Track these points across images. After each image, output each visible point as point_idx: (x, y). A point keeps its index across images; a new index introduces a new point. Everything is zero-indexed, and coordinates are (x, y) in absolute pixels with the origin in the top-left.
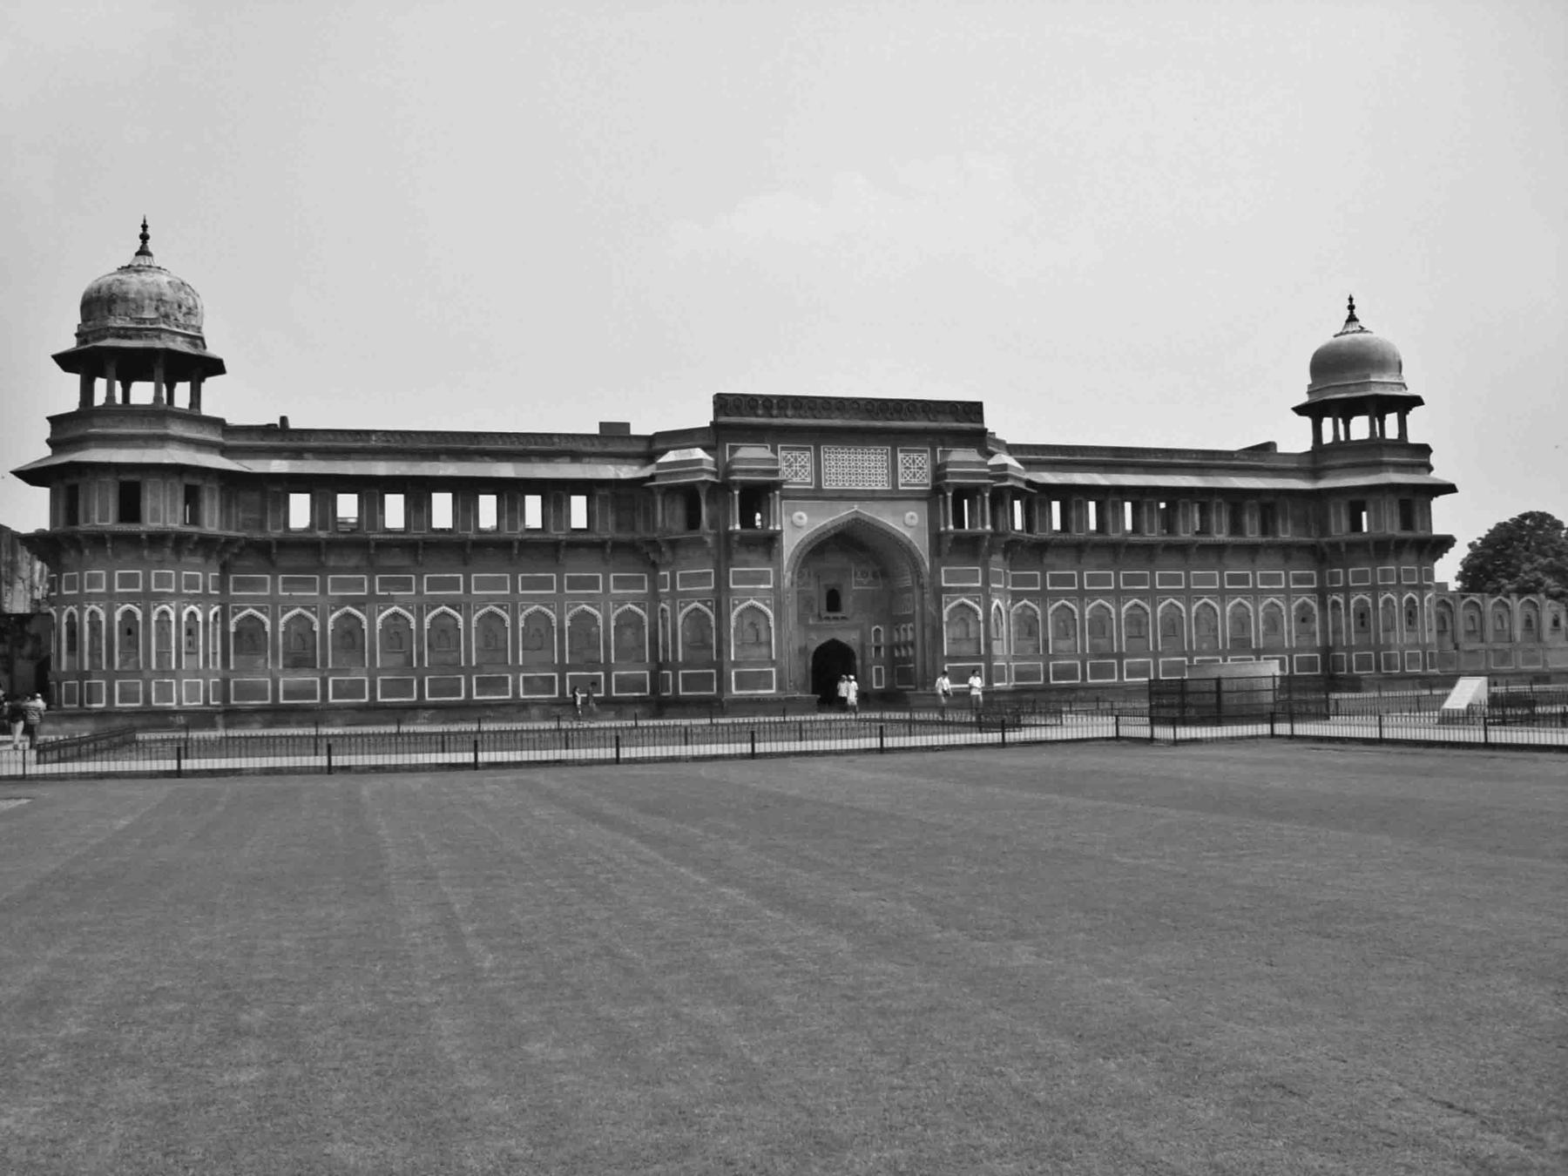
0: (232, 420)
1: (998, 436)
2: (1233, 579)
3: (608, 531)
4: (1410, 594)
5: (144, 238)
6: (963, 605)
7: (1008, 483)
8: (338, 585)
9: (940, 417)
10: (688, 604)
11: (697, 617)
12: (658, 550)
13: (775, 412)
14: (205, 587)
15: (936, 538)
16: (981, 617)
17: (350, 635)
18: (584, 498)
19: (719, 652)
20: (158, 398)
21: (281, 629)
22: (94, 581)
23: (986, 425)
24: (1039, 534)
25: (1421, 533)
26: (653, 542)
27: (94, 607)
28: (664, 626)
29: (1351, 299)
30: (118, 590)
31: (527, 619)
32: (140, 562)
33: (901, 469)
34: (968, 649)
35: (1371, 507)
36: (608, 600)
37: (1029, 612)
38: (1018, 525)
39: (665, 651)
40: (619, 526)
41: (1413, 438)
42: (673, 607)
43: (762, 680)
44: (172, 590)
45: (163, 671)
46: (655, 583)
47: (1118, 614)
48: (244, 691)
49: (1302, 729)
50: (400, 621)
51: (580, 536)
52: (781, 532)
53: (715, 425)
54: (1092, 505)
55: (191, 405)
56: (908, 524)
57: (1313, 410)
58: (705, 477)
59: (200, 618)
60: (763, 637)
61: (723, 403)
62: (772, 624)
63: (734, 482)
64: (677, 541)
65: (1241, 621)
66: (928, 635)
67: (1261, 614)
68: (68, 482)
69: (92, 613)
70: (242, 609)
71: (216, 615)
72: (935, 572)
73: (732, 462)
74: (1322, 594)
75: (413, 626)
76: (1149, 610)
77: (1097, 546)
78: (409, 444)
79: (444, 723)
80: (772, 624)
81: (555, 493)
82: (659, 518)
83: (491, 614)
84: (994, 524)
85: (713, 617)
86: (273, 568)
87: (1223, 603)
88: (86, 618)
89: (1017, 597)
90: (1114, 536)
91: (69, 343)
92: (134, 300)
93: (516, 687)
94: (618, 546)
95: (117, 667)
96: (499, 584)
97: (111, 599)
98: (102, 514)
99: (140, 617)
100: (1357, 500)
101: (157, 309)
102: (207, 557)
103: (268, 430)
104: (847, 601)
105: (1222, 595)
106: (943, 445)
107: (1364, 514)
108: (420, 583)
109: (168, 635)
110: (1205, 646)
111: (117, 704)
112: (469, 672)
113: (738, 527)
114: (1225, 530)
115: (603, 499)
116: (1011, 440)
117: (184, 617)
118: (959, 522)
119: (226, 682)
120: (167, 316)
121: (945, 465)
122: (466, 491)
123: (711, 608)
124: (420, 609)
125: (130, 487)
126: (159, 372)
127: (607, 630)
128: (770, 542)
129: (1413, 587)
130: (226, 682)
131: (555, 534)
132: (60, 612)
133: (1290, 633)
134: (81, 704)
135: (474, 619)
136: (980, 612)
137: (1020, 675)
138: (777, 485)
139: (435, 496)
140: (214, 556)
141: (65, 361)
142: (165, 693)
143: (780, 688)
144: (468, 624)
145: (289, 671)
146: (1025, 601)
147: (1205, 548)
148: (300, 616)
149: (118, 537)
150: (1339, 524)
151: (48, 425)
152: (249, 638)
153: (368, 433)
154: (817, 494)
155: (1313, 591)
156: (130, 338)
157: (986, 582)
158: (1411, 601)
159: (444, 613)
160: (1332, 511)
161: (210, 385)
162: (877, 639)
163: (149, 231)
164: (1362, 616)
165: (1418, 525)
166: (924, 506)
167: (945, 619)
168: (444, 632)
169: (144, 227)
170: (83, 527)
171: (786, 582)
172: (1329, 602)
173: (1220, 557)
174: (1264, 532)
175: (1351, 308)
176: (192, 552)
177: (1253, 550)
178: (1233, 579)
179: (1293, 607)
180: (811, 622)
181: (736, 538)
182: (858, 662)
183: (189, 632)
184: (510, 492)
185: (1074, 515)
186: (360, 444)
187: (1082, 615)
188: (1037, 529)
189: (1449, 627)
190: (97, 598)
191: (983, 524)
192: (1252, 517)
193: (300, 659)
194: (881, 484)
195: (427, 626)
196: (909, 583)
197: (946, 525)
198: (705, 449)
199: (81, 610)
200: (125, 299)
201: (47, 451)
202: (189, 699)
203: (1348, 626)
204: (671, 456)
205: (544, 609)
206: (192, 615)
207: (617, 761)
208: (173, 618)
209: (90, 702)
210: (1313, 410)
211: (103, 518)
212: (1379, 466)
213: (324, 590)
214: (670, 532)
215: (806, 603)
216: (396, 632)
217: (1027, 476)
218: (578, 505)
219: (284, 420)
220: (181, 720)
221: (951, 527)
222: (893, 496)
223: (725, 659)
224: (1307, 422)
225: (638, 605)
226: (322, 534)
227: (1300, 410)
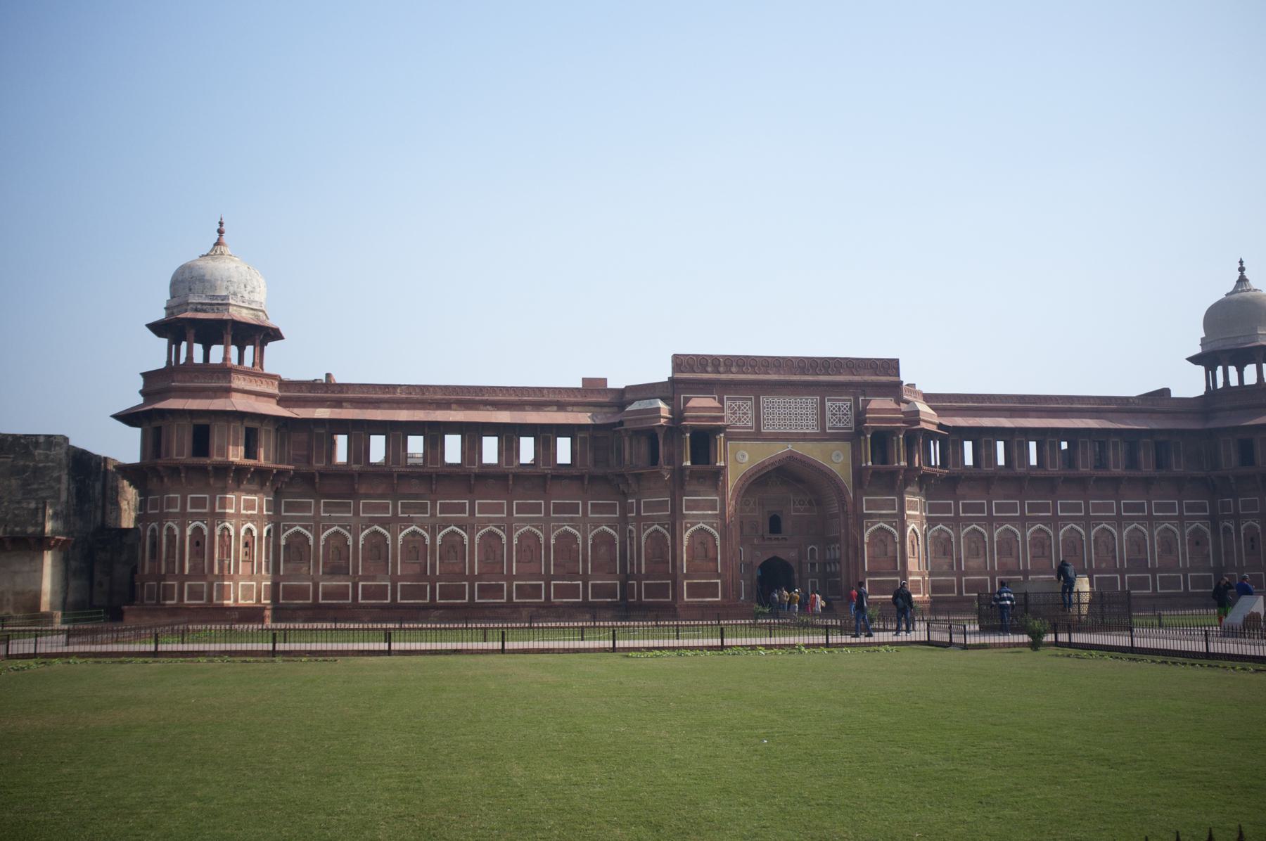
0: (285, 376)
1: (917, 388)
2: (1128, 508)
5: (221, 232)
6: (881, 529)
7: (923, 425)
8: (368, 508)
10: (650, 526)
11: (656, 538)
13: (721, 369)
14: (261, 509)
15: (858, 473)
16: (897, 540)
17: (377, 548)
19: (674, 566)
20: (225, 358)
21: (322, 543)
22: (171, 503)
23: (902, 378)
26: (622, 476)
27: (170, 523)
28: (631, 545)
29: (1241, 262)
30: (189, 510)
31: (519, 538)
33: (827, 412)
36: (585, 524)
37: (944, 535)
39: (632, 564)
43: (711, 590)
44: (232, 511)
45: (222, 577)
46: (625, 509)
47: (1024, 536)
48: (291, 592)
49: (1078, 638)
50: (417, 538)
51: (563, 471)
52: (725, 467)
57: (1207, 360)
58: (663, 421)
59: (255, 534)
60: (711, 554)
61: (679, 362)
62: (718, 543)
64: (641, 474)
65: (1138, 543)
66: (851, 554)
67: (1156, 539)
68: (156, 424)
69: (170, 529)
71: (269, 531)
72: (857, 502)
73: (686, 409)
74: (1214, 520)
75: (428, 542)
77: (1004, 479)
78: (427, 396)
79: (449, 622)
80: (718, 543)
81: (545, 436)
82: (627, 456)
83: (491, 533)
84: (910, 460)
86: (319, 495)
87: (1120, 528)
88: (165, 532)
90: (1019, 470)
91: (161, 315)
92: (209, 281)
93: (510, 592)
94: (594, 479)
95: (187, 572)
96: (498, 508)
97: (184, 518)
98: (180, 448)
99: (206, 532)
101: (227, 288)
102: (262, 485)
103: (313, 385)
104: (786, 525)
105: (1119, 521)
110: (1103, 565)
111: (186, 602)
112: (472, 578)
113: (689, 463)
117: (242, 533)
121: (865, 411)
122: (472, 434)
124: (433, 528)
125: (202, 430)
127: (585, 548)
128: (716, 477)
130: (275, 586)
131: (542, 468)
132: (145, 528)
133: (1184, 554)
134: (158, 601)
135: (477, 537)
136: (897, 535)
137: (935, 588)
138: (720, 429)
139: (447, 437)
141: (158, 328)
142: (223, 591)
143: (724, 596)
144: (472, 541)
147: (1099, 480)
148: (337, 533)
149: (190, 469)
152: (297, 549)
153: (395, 387)
154: (757, 435)
155: (1204, 518)
156: (205, 311)
159: (453, 532)
161: (271, 348)
162: (812, 557)
163: (224, 227)
164: (1252, 540)
166: (847, 446)
167: (866, 540)
168: (453, 547)
169: (221, 224)
174: (1159, 466)
175: (1242, 269)
176: (250, 481)
177: (1148, 482)
178: (1128, 508)
179: (1187, 532)
180: (756, 542)
181: (688, 472)
182: (796, 576)
183: (246, 545)
184: (509, 435)
185: (983, 452)
187: (991, 537)
188: (950, 466)
190: (174, 516)
193: (336, 569)
194: (812, 429)
195: (439, 541)
198: (663, 399)
199: (161, 526)
201: (140, 400)
202: (244, 598)
203: (1239, 550)
204: (635, 406)
206: (249, 531)
207: (503, 651)
208: (232, 533)
209: (165, 599)
211: (180, 453)
213: (357, 513)
216: (414, 547)
219: (328, 375)
220: (236, 615)
221: (870, 463)
222: (823, 436)
224: (1201, 369)
225: (610, 527)
226: (356, 467)
227: (1195, 360)
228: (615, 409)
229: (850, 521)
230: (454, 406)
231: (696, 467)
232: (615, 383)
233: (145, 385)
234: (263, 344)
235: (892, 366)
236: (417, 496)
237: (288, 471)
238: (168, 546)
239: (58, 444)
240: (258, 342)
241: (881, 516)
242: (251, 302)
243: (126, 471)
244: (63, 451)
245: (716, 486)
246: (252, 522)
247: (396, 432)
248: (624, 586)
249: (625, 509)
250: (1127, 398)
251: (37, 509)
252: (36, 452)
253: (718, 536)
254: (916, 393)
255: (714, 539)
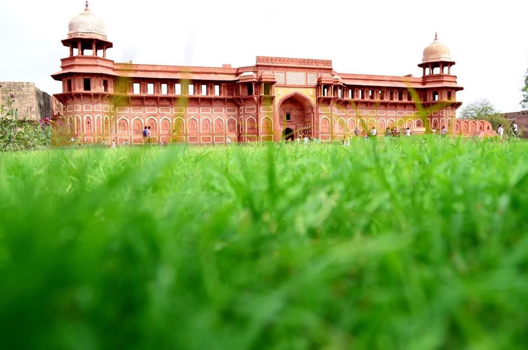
3: (225, 95)
4: (449, 118)
5: (87, 6)
6: (325, 118)
7: (339, 83)
9: (320, 64)
10: (248, 116)
12: (241, 102)
13: (273, 62)
15: (318, 100)
16: (330, 122)
18: (218, 86)
20: (93, 54)
21: (132, 122)
23: (332, 67)
24: (345, 99)
25: (452, 101)
26: (239, 100)
30: (84, 110)
32: (93, 103)
33: (308, 79)
34: (326, 130)
35: (439, 93)
38: (340, 96)
39: (242, 130)
40: (228, 94)
41: (452, 74)
42: (244, 118)
44: (101, 111)
52: (275, 97)
53: (257, 66)
54: (360, 91)
55: (104, 56)
56: (309, 94)
57: (423, 66)
58: (254, 80)
59: (109, 119)
60: (270, 126)
61: (258, 59)
63: (262, 82)
68: (68, 78)
69: (77, 117)
70: (121, 117)
76: (375, 121)
80: (272, 122)
84: (334, 95)
85: (256, 120)
88: (75, 119)
89: (339, 116)
91: (66, 37)
94: (229, 100)
98: (79, 89)
99: (91, 118)
100: (436, 91)
101: (93, 27)
102: (110, 101)
103: (126, 64)
106: (320, 72)
107: (437, 97)
108: (172, 110)
109: (100, 123)
113: (263, 94)
114: (398, 99)
115: (224, 86)
116: (339, 72)
118: (324, 95)
119: (116, 138)
120: (96, 29)
121: (321, 78)
123: (255, 118)
124: (172, 117)
126: (94, 46)
127: (225, 124)
129: (450, 116)
132: (67, 117)
138: (274, 83)
140: (112, 101)
141: (65, 43)
144: (186, 121)
145: (135, 135)
146: (341, 118)
149: (84, 95)
150: (430, 98)
151: (61, 62)
153: (156, 66)
154: (285, 86)
157: (331, 112)
158: (449, 120)
160: (428, 94)
161: (108, 50)
165: (452, 99)
166: (315, 89)
169: (87, 2)
170: (73, 92)
171: (276, 111)
172: (426, 120)
173: (396, 107)
177: (405, 105)
180: (282, 122)
181: (263, 98)
183: (106, 123)
185: (355, 94)
186: (153, 69)
189: (459, 128)
190: (79, 113)
191: (331, 95)
192: (405, 96)
194: (303, 83)
196: (310, 112)
197: (321, 95)
198: (254, 72)
199: (74, 117)
200: (83, 24)
201: (61, 69)
205: (207, 118)
208: (101, 118)
210: (423, 66)
212: (442, 81)
213: (144, 112)
214: (244, 96)
215: (281, 117)
216: (166, 124)
217: (343, 82)
218: (217, 87)
219: (131, 61)
221: (322, 96)
223: (259, 132)
224: (421, 69)
225: (234, 117)
227: (420, 66)
228: (235, 76)
229: (315, 116)
230: (178, 73)
231: (266, 96)
232: (236, 65)
233: (62, 64)
234: (106, 49)
235: (329, 62)
236: (166, 106)
237: (120, 96)
238: (77, 124)
239: (31, 86)
240: (104, 48)
241: (325, 114)
242: (102, 32)
243: (57, 96)
244: (33, 89)
245: (272, 103)
246: (107, 115)
247: (157, 82)
248: (238, 137)
249: (238, 110)
250: (400, 77)
251: (28, 110)
252: (23, 89)
253: (272, 120)
254: (335, 72)
255: (271, 121)
